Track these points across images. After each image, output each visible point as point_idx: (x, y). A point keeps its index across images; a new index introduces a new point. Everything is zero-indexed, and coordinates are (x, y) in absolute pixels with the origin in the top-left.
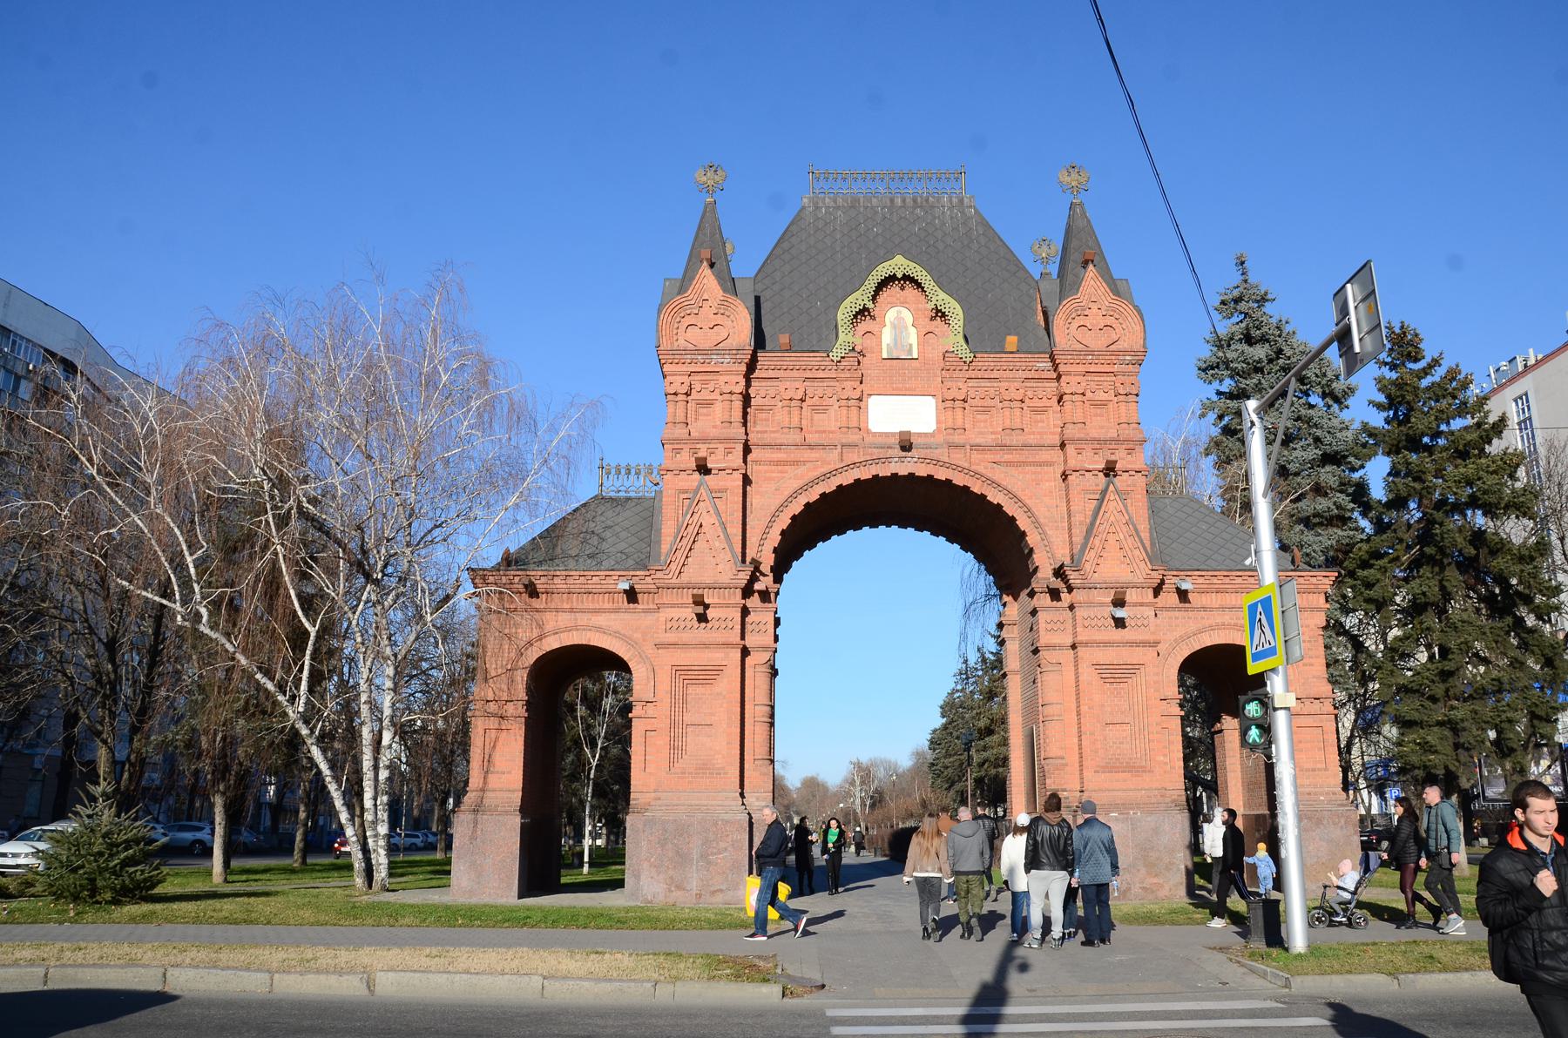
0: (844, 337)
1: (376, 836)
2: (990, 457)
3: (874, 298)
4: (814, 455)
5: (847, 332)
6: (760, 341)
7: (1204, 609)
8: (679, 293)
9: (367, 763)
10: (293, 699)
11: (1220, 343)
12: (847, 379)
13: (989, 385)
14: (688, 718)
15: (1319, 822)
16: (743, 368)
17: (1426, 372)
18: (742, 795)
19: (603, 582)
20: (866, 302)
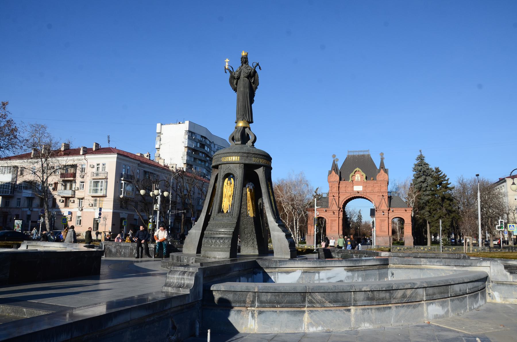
0: (351, 179)
1: (297, 238)
2: (369, 194)
3: (354, 173)
4: (347, 194)
6: (340, 179)
7: (395, 212)
9: (295, 230)
10: (287, 223)
11: (415, 165)
14: (333, 225)
15: (408, 239)
16: (338, 183)
17: (441, 174)
18: (339, 234)
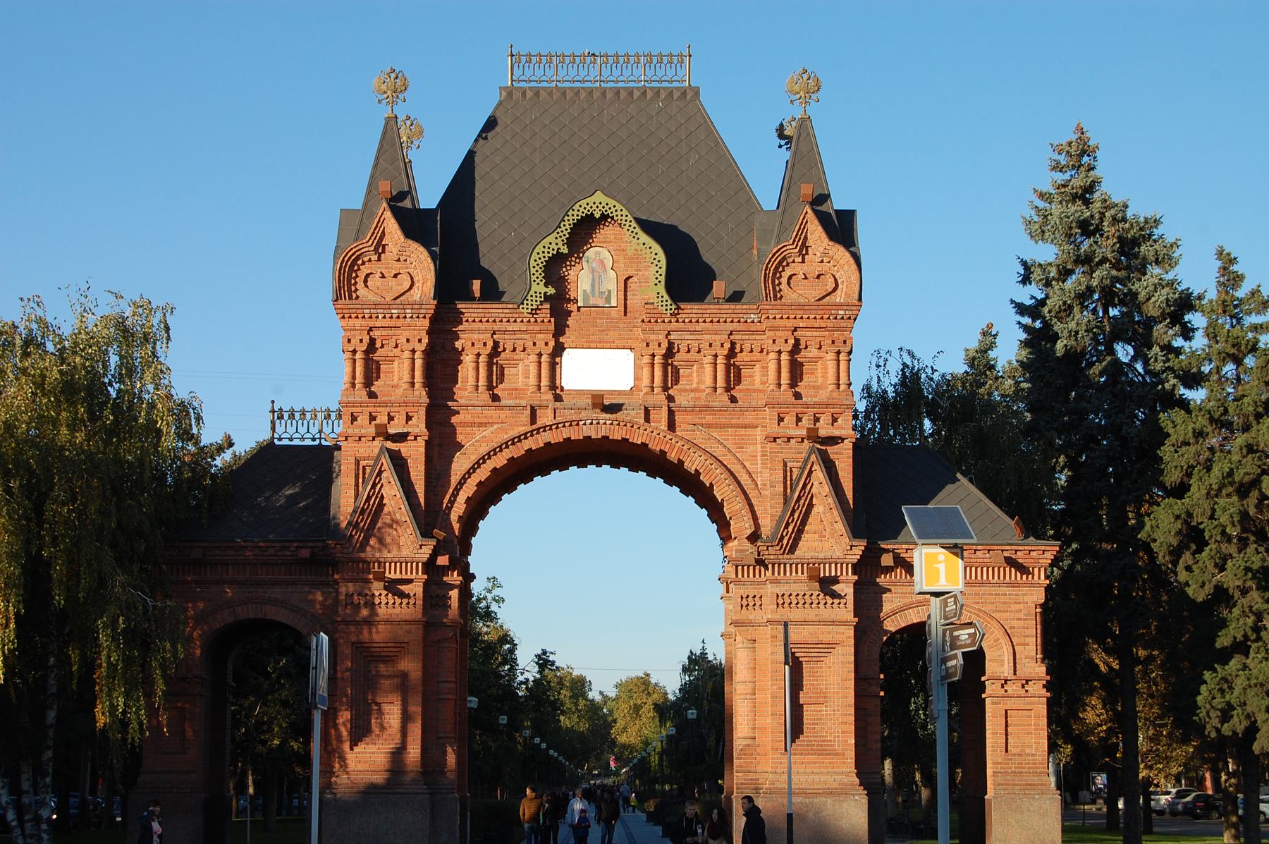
5: (538, 281)
8: (356, 240)
12: (540, 332)
13: (690, 337)
19: (279, 553)
20: (560, 246)
